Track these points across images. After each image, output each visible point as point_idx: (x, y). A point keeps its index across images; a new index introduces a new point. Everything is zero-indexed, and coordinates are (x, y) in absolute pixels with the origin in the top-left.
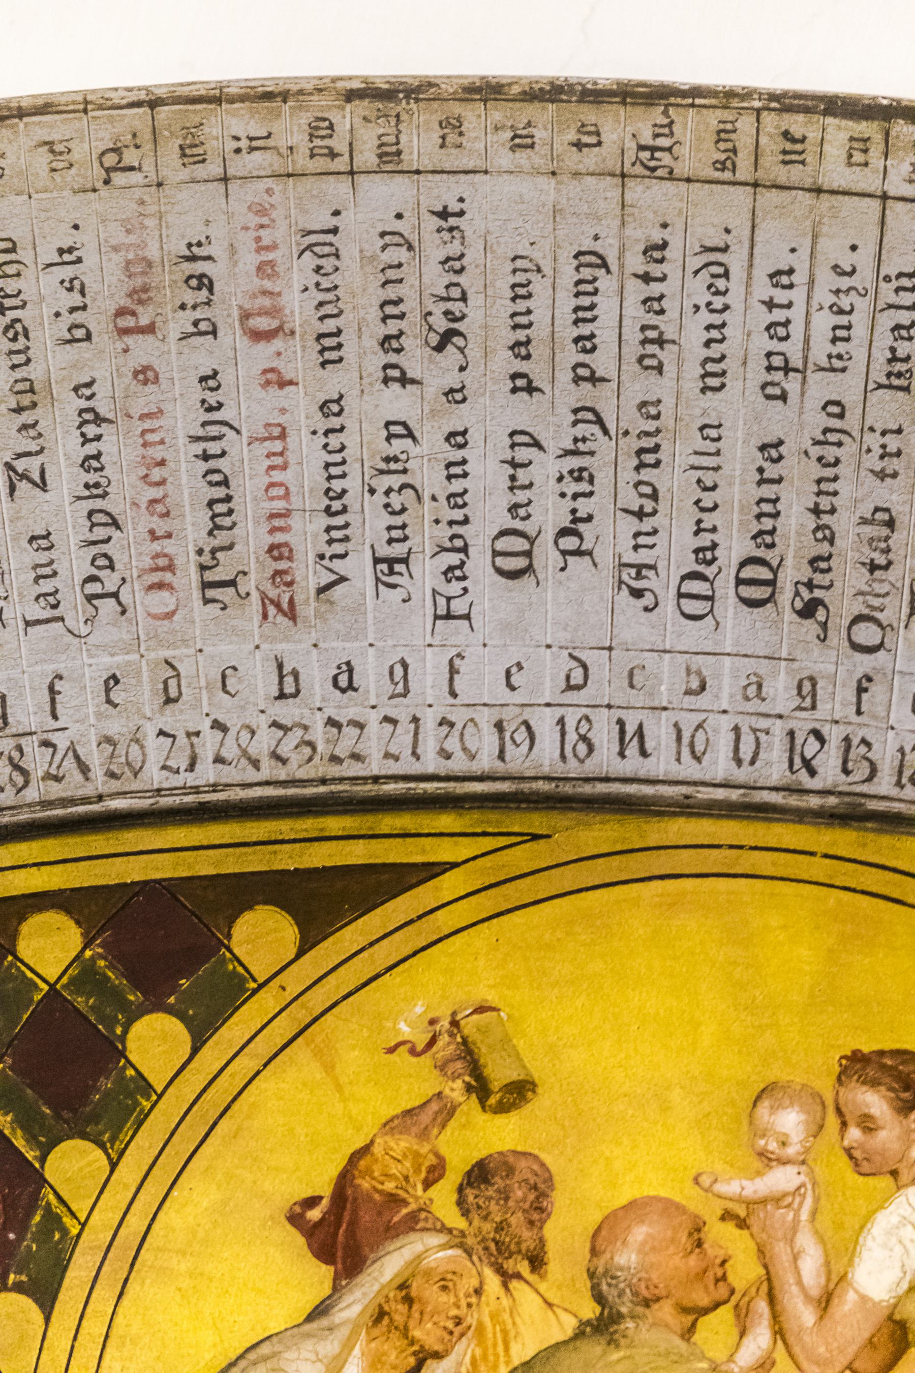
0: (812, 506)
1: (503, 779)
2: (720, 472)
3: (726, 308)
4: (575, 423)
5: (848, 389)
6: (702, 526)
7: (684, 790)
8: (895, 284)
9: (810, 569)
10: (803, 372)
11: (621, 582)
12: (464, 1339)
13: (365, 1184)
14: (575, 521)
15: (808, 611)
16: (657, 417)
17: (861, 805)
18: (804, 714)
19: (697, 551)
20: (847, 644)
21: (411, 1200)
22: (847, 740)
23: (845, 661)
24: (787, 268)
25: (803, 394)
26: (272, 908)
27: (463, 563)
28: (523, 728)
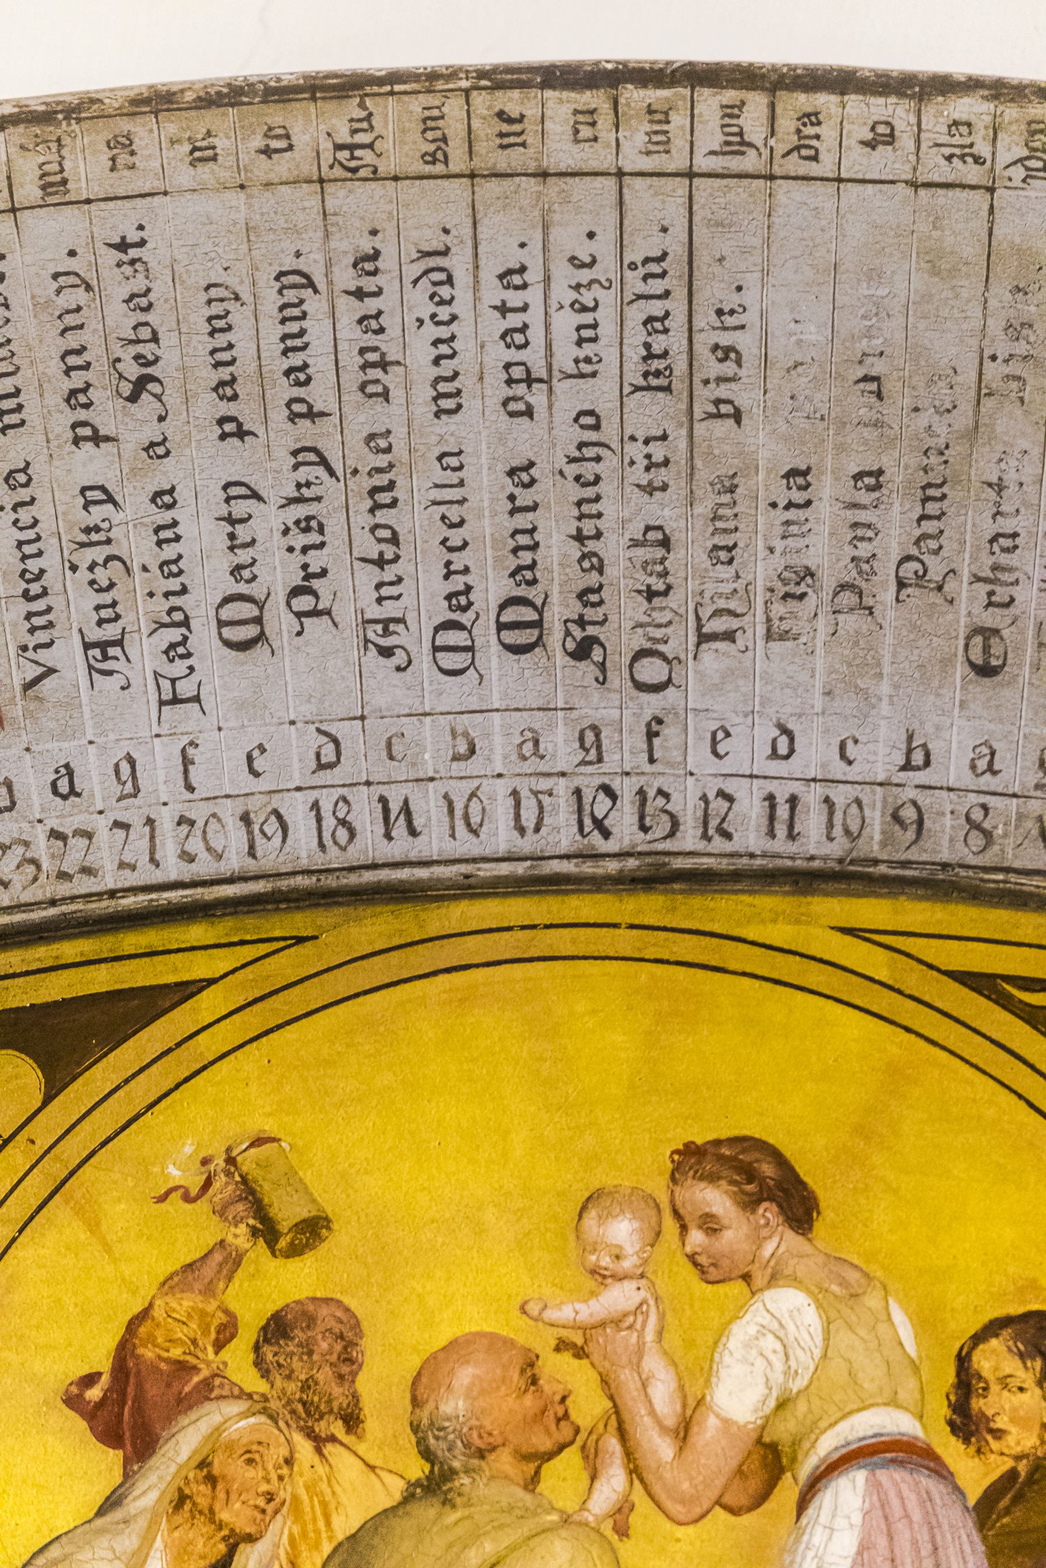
0: (575, 533)
1: (257, 878)
2: (466, 505)
3: (454, 318)
4: (296, 467)
5: (601, 394)
6: (452, 568)
7: (463, 868)
8: (641, 271)
9: (579, 604)
10: (548, 382)
11: (367, 641)
12: (279, 1517)
13: (148, 1353)
14: (307, 577)
15: (582, 652)
16: (388, 450)
17: (665, 864)
18: (589, 769)
19: (449, 597)
20: (630, 684)
21: (202, 1366)
22: (641, 793)
23: (630, 704)
24: (518, 266)
25: (550, 407)
26: (10, 1052)
27: (185, 639)
28: (273, 818)
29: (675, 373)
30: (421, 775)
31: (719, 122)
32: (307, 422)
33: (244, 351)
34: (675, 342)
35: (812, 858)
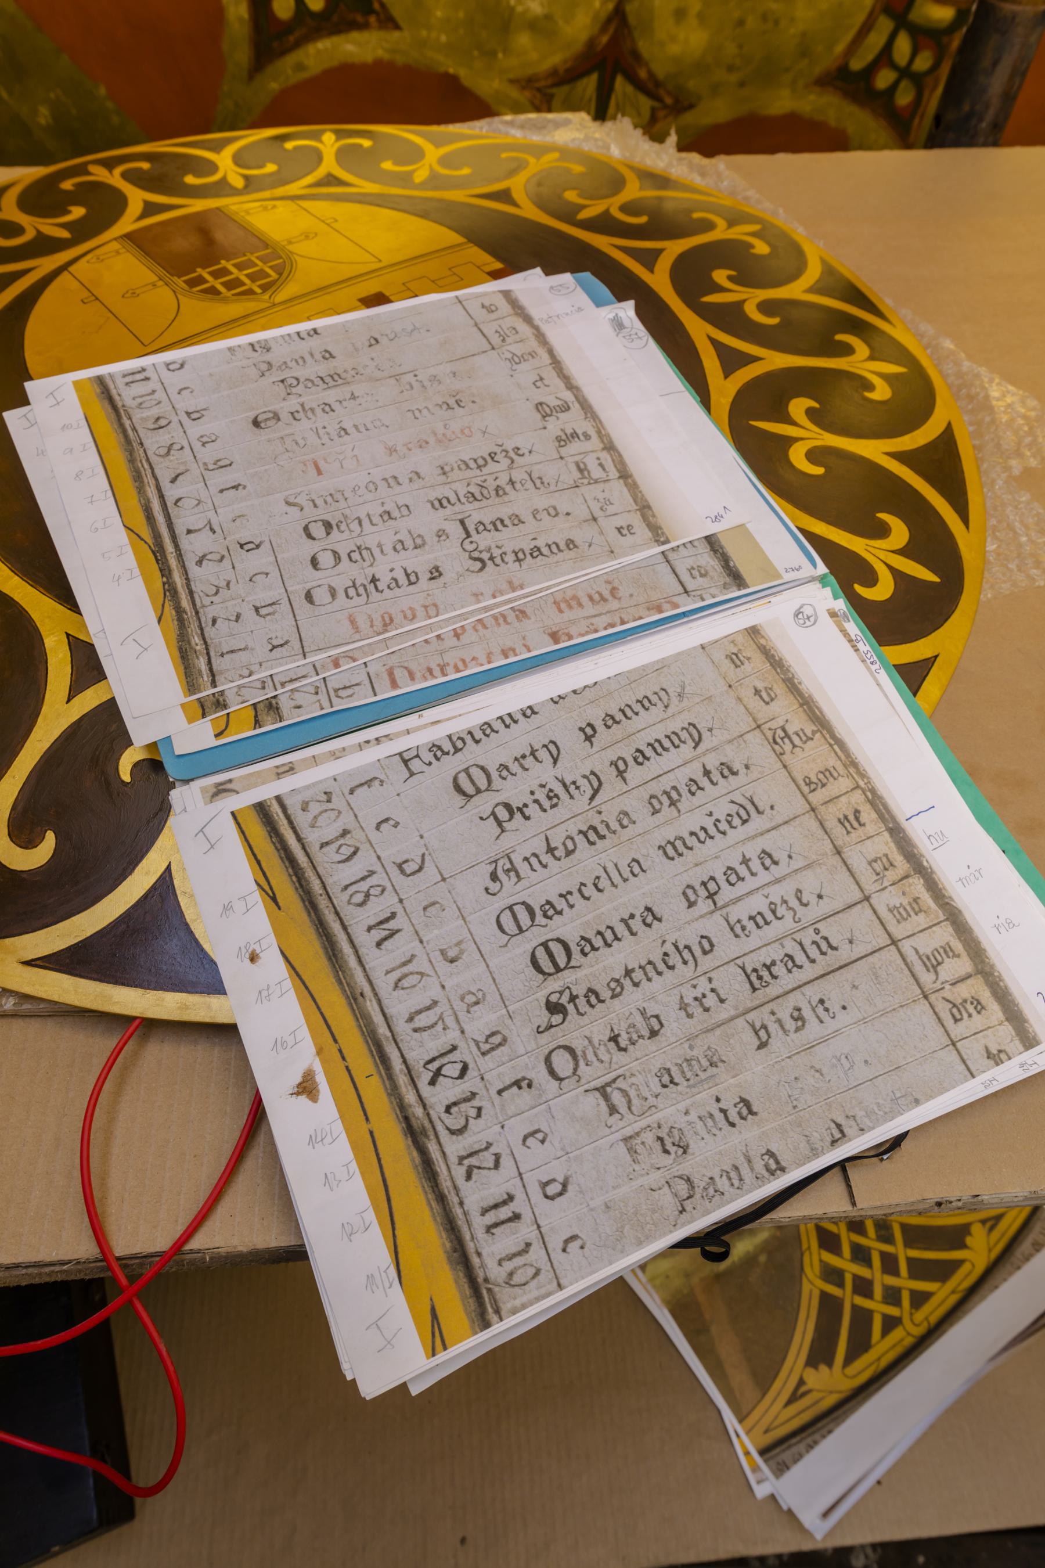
0: (630, 968)
1: (308, 855)
2: (613, 889)
3: (724, 833)
4: (585, 777)
5: (727, 947)
6: (569, 897)
7: (367, 990)
8: (817, 938)
9: (585, 992)
10: (717, 908)
11: (496, 861)
14: (519, 809)
15: (554, 1008)
16: (623, 827)
17: (427, 1137)
18: (474, 1049)
19: (548, 902)
20: (547, 1052)
22: (474, 1095)
23: (532, 1059)
24: (776, 859)
25: (702, 917)
27: (448, 753)
28: (352, 849)
29: (767, 989)
30: (421, 933)
31: (937, 946)
32: (615, 773)
33: (637, 723)
34: (787, 980)
35: (479, 1254)
